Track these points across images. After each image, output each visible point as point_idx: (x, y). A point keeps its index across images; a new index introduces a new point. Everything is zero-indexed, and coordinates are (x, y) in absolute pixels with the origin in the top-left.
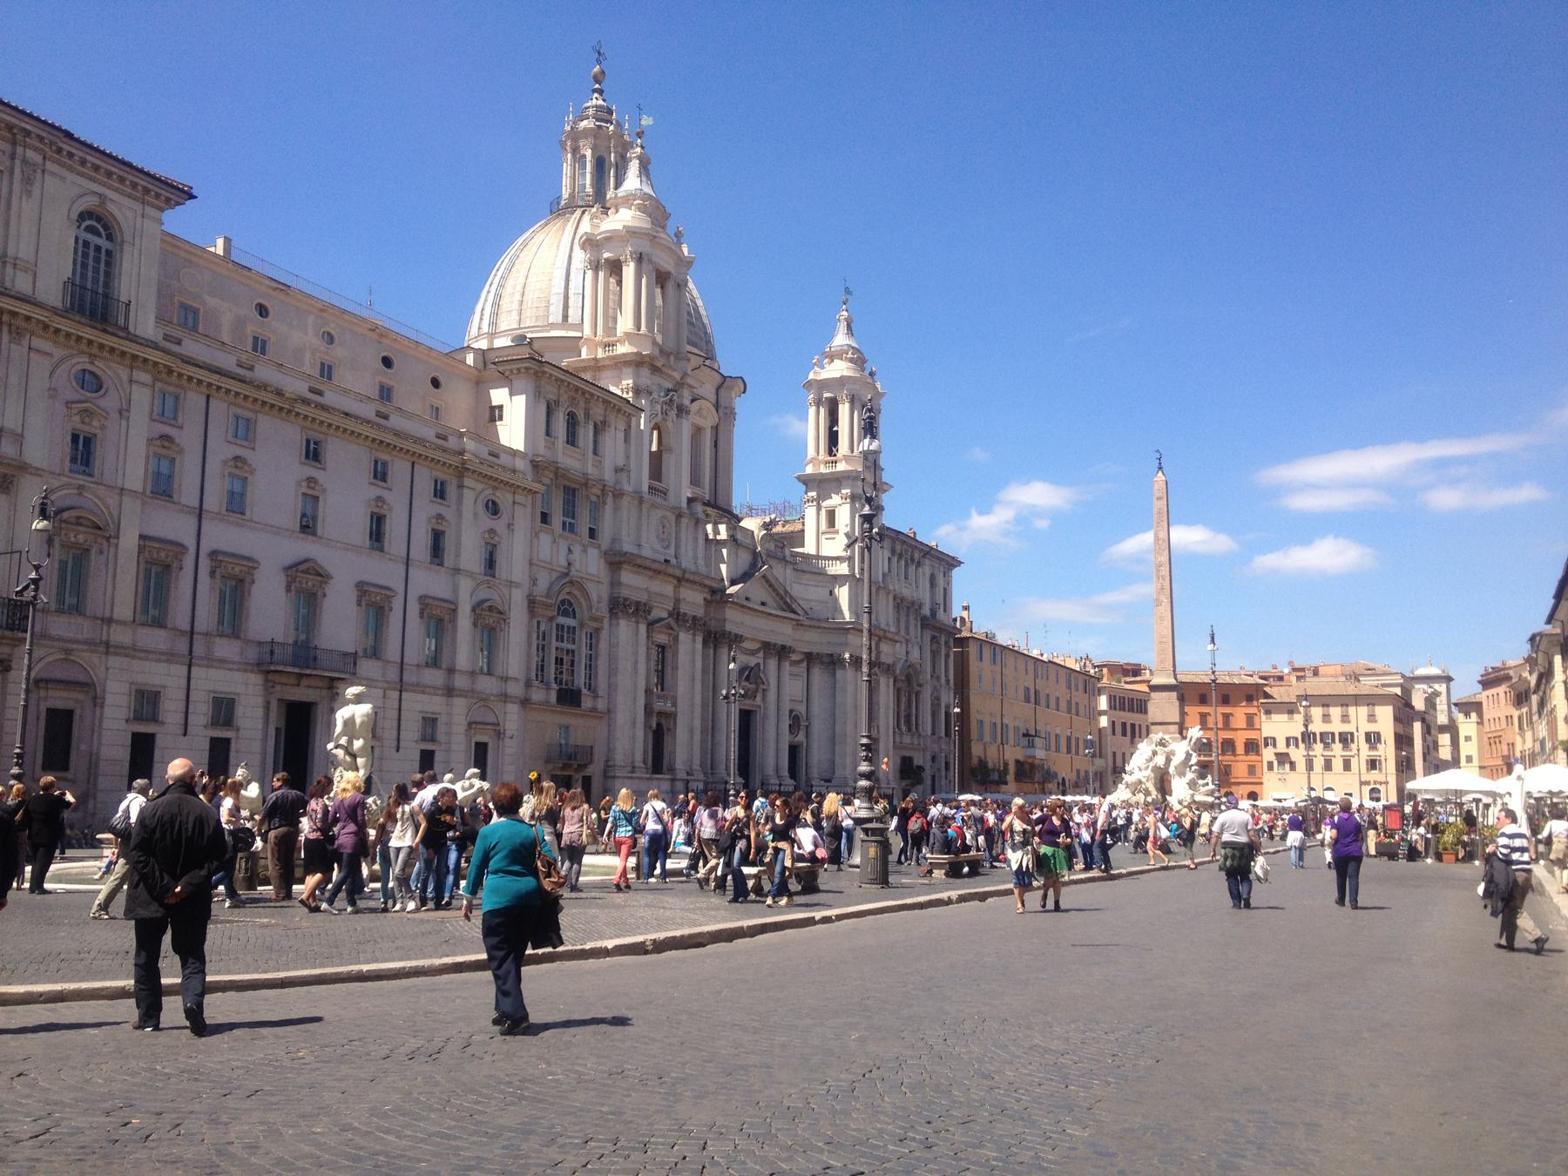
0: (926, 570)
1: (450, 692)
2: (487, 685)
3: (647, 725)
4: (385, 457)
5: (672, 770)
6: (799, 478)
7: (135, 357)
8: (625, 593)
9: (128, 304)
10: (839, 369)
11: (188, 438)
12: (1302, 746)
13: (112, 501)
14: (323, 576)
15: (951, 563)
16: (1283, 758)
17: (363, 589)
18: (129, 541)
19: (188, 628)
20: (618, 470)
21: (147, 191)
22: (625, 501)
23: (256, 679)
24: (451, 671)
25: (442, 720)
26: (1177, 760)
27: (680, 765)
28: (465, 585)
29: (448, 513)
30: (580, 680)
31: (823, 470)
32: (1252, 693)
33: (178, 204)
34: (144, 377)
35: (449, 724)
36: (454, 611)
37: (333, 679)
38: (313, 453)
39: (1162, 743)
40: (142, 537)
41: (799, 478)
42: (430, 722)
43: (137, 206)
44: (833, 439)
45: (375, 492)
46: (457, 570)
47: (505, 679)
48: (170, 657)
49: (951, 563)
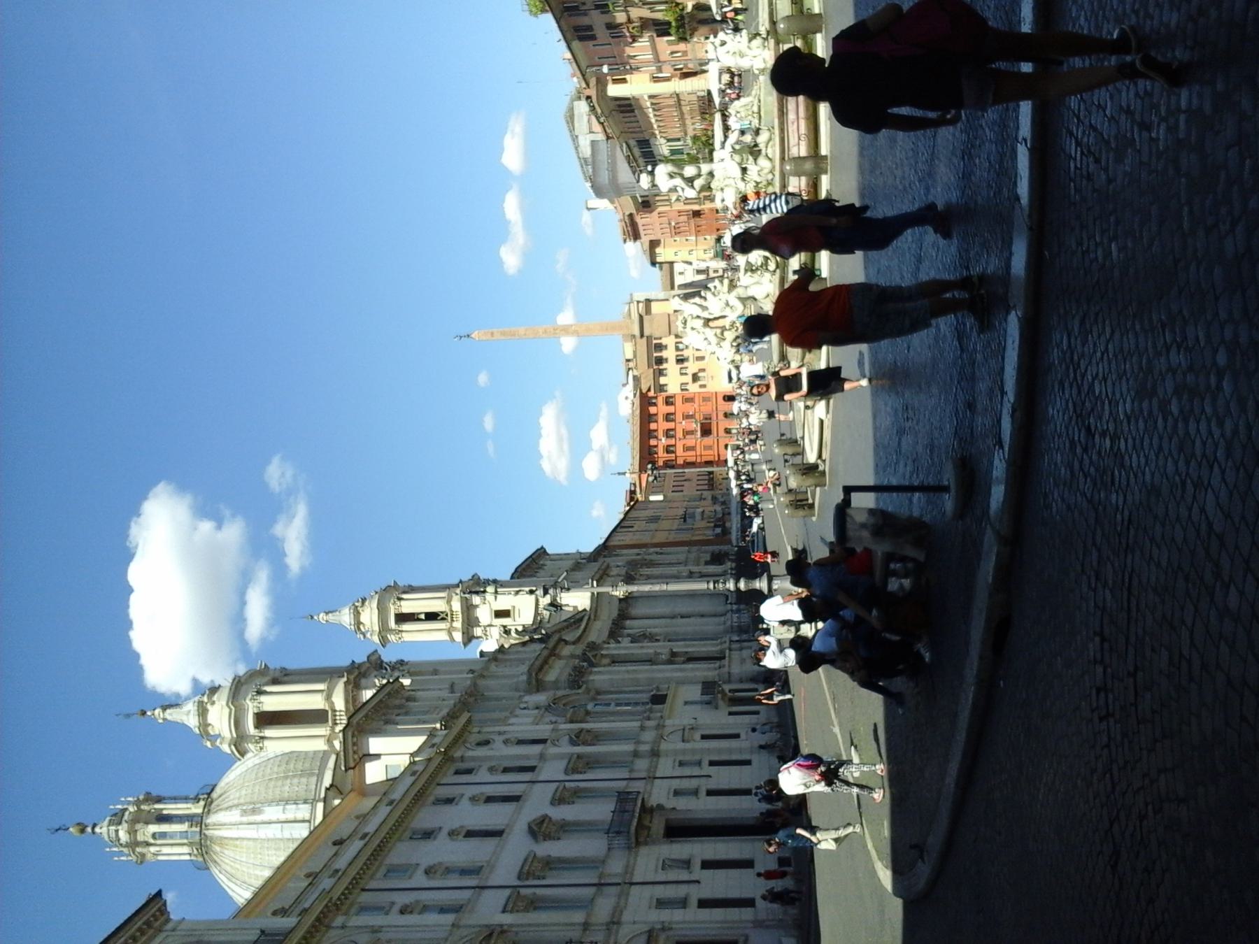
0: (548, 563)
1: (655, 754)
2: (649, 736)
3: (684, 663)
4: (432, 798)
5: (723, 652)
6: (465, 644)
7: (318, 919)
8: (564, 677)
9: (263, 932)
10: (369, 617)
11: (402, 899)
12: (686, 364)
13: (464, 932)
14: (544, 819)
15: (541, 552)
16: (695, 378)
17: (558, 800)
18: (507, 919)
19: (592, 890)
20: (452, 692)
21: (148, 923)
22: (481, 682)
23: (644, 850)
24: (636, 754)
25: (681, 758)
26: (698, 311)
27: (719, 648)
28: (552, 750)
29: (486, 765)
30: (645, 697)
31: (458, 624)
32: (645, 401)
33: (165, 904)
34: (339, 921)
35: (684, 752)
36: (579, 756)
37: (644, 808)
38: (428, 835)
39: (685, 323)
40: (504, 911)
41: (465, 644)
42: (681, 764)
43: (163, 935)
44: (432, 616)
45: (465, 803)
46: (542, 757)
47: (642, 728)
48: (623, 895)
49: (541, 552)
